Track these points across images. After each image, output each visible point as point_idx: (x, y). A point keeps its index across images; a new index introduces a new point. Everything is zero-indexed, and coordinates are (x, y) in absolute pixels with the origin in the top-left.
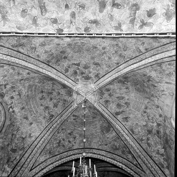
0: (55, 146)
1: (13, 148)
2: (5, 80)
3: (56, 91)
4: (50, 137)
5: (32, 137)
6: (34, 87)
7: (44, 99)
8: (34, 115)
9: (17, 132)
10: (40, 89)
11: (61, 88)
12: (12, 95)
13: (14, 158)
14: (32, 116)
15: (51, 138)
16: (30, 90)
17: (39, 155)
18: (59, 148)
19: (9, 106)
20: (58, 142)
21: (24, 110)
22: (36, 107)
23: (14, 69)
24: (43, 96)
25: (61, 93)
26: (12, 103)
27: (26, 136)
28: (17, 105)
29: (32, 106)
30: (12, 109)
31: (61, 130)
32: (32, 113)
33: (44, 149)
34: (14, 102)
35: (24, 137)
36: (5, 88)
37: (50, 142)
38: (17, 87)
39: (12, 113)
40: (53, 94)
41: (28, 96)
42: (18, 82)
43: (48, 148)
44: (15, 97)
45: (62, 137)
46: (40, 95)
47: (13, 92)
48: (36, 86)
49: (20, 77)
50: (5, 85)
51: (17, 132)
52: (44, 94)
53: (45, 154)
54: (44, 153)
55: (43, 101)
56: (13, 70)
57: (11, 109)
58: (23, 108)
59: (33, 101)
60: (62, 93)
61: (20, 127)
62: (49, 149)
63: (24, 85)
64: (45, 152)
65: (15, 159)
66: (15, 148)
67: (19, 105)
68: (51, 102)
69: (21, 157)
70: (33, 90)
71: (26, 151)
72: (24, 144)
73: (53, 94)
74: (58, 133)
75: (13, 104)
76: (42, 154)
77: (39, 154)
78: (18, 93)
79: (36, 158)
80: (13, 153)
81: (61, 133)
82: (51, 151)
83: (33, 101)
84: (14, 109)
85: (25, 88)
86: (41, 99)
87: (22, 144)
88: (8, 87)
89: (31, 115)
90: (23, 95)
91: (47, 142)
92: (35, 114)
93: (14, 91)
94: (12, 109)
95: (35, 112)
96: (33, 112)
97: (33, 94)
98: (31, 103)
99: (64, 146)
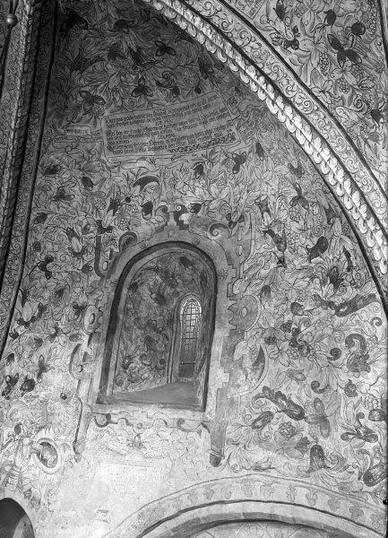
0: (351, 79)
1: (311, 246)
2: (85, 230)
3: (111, 41)
4: (300, 97)
5: (300, 166)
6: (121, 129)
7: (172, 77)
8: (234, 129)
9: (268, 211)
10: (126, 101)
11: (86, 28)
12: (140, 208)
13: (344, 257)
14: (237, 138)
15: (310, 92)
16: (132, 141)
17: (368, 168)
18: (365, 62)
19: (172, 222)
20: (335, 56)
21: (207, 167)
22: (206, 112)
23: (42, 217)
24: (158, 84)
25: (114, 17)
26: (165, 209)
27: (294, 185)
28: (177, 194)
29: (200, 128)
30: (184, 210)
31: (280, 26)
32: (225, 133)
33: (349, 139)
34: (164, 204)
35: (295, 194)
36: (110, 229)
37: (325, 99)
38: (117, 190)
39: (199, 214)
40: (138, 48)
41: (157, 147)
42: (95, 189)
43: (354, 117)
44: (148, 198)
45: (317, 22)
46: (159, 95)
47: (131, 203)
48: (110, 123)
49: (76, 189)
50: (101, 229)
51: (268, 211)
52: (150, 81)
53: (376, 140)
54: (371, 142)
55: (180, 81)
56: (49, 216)
57: (185, 217)
58: (199, 169)
59: (181, 124)
60: (112, 11)
61: (258, 193)
62: (361, 115)
63: (109, 169)
64: (366, 141)
65: (348, 255)
66: (315, 240)
67: (180, 185)
68: (178, 49)
69: (353, 234)
70: (135, 127)
71: (340, 210)
72: (318, 203)
73: (138, 48)
74: (294, 44)
75: (169, 206)
76: (367, 152)
77: (365, 169)
78: (139, 187)
79: (376, 186)
80: (326, 254)
81: (297, 21)
82: (373, 107)
83: (181, 124)
84: (187, 204)
85: (120, 165)
86: (176, 91)
87: (316, 210)
88: (109, 219)
89: (233, 138)
90: (150, 167)
91: (322, 113)
92: (229, 124)
93: (128, 200)
94: (184, 210)
95: (223, 122)
96: (223, 127)
97: (152, 125)
98: (187, 132)
99: (357, 29)
